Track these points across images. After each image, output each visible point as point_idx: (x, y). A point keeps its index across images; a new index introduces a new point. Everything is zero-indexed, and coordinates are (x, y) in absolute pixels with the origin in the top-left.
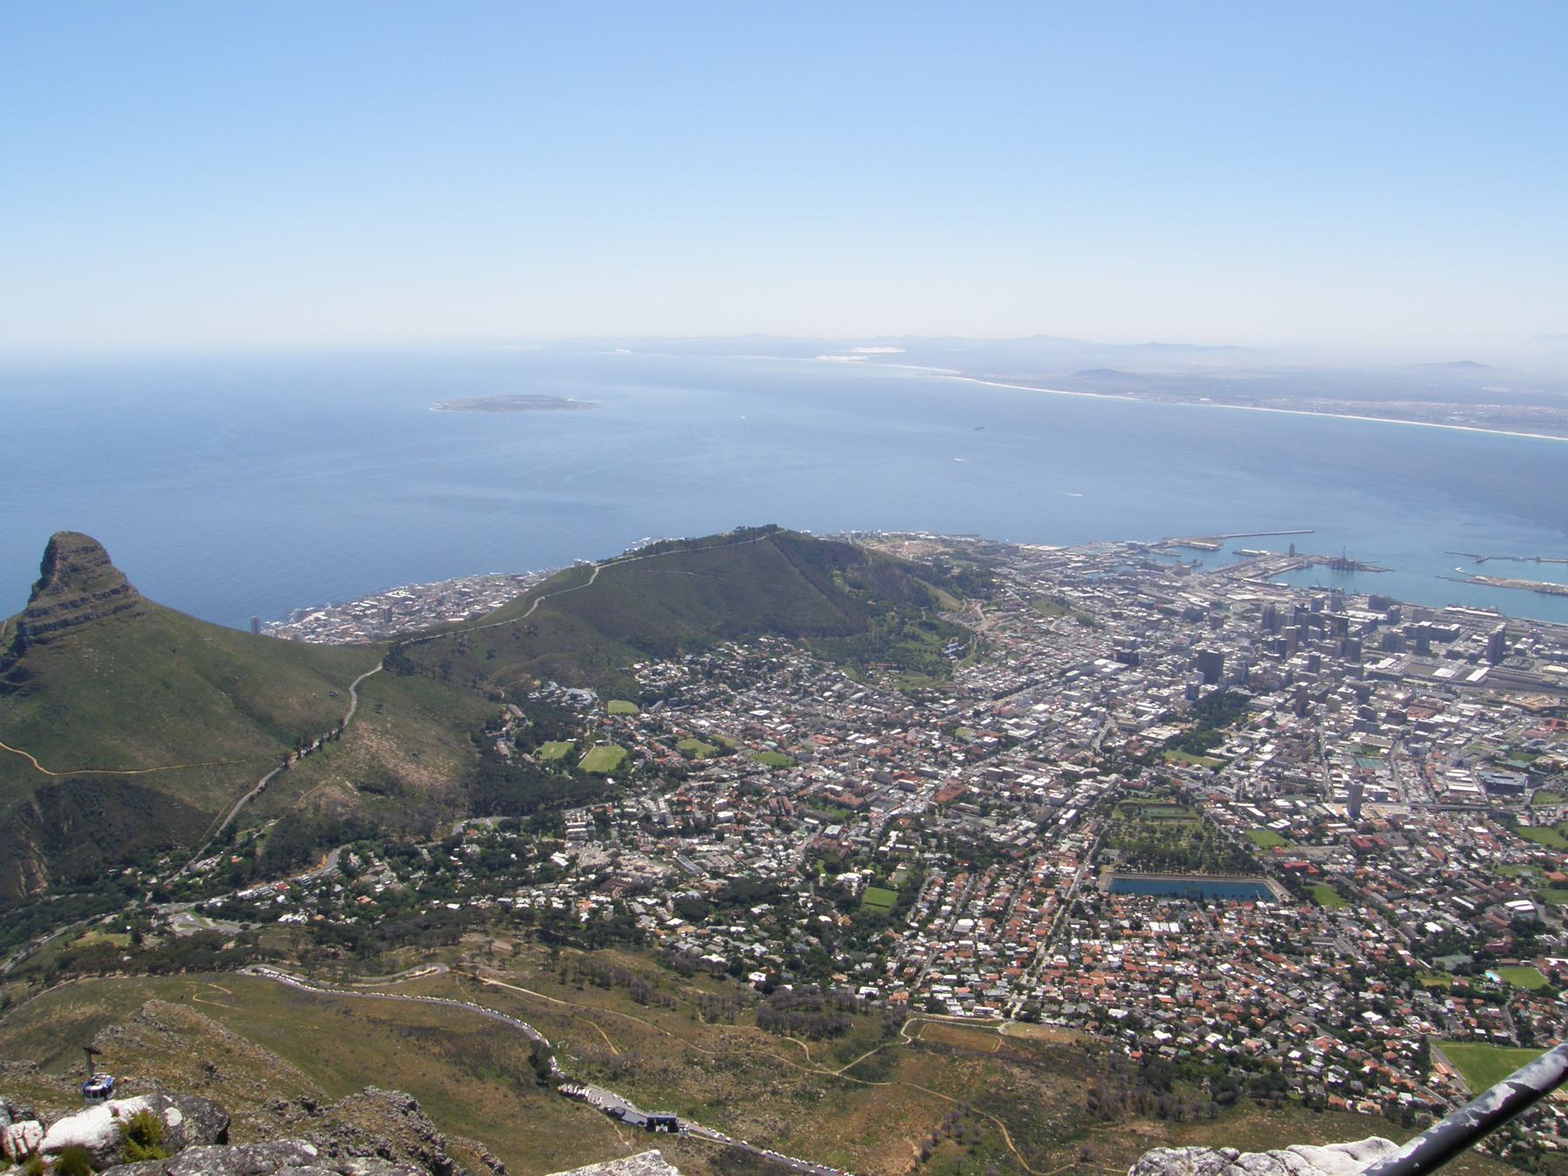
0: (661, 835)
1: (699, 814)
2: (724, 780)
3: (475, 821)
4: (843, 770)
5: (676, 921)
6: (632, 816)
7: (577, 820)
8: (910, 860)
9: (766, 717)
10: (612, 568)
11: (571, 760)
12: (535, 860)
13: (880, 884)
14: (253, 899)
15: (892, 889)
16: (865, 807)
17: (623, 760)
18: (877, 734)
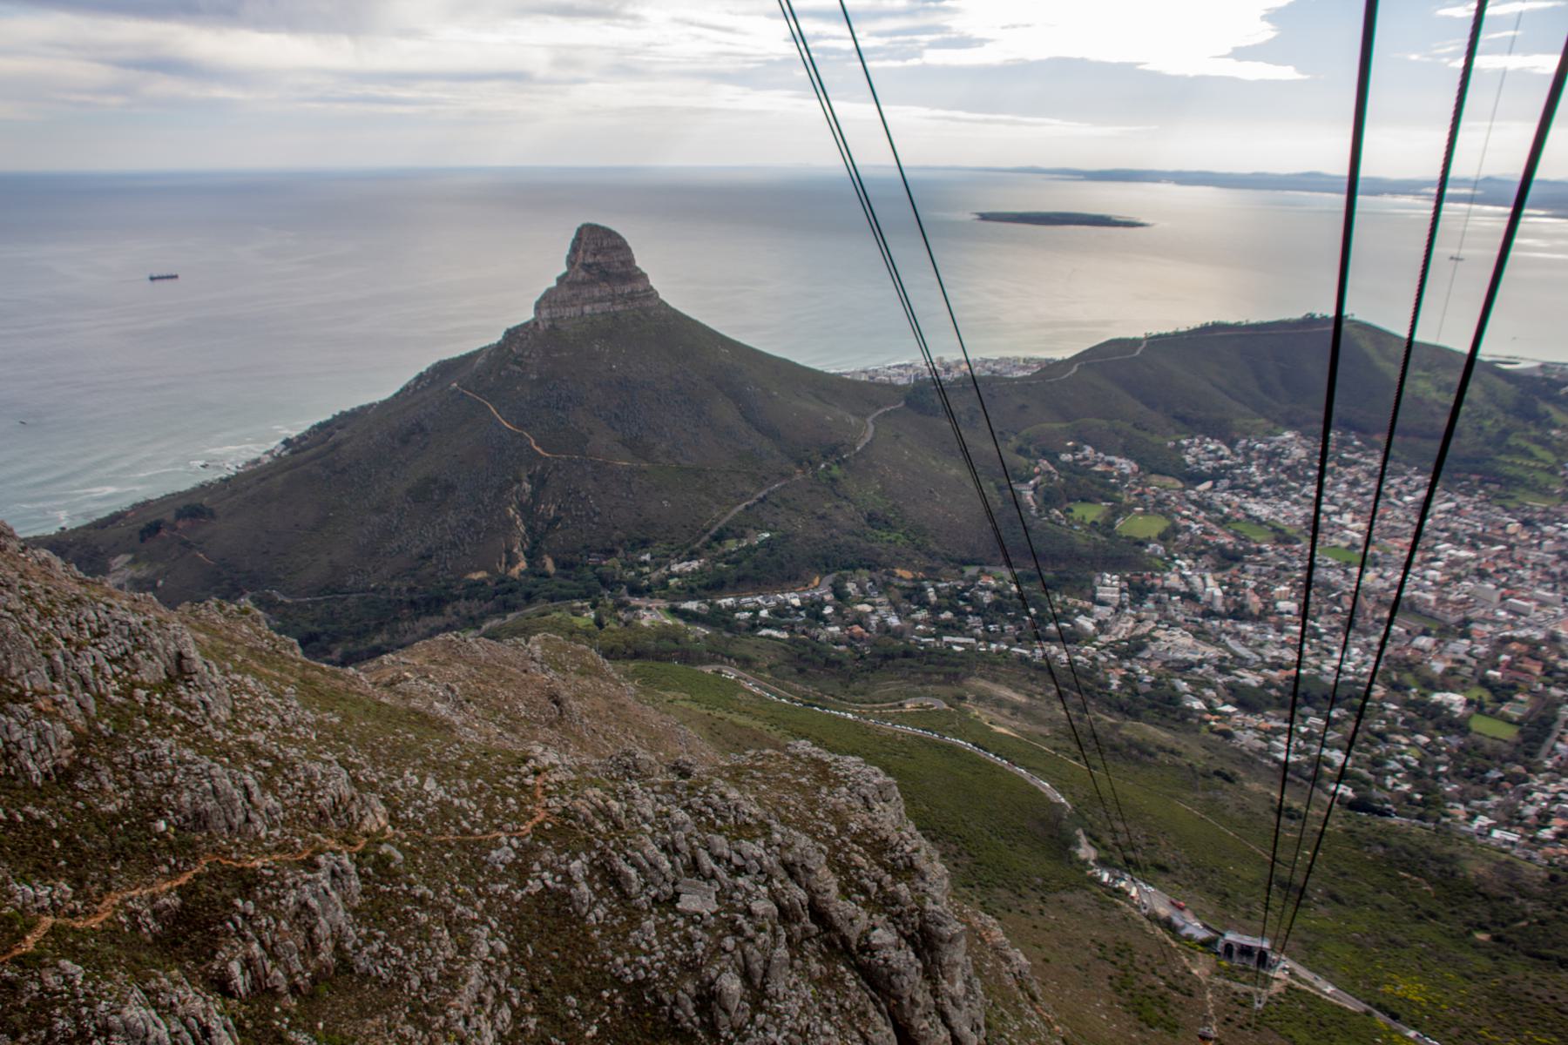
0: (1209, 614)
1: (1256, 599)
2: (1285, 568)
3: (987, 569)
4: (1435, 583)
5: (1229, 709)
6: (1172, 591)
7: (1110, 586)
8: (1530, 692)
9: (1334, 513)
10: (1158, 342)
11: (1107, 527)
12: (1056, 619)
13: (1493, 714)
14: (733, 610)
15: (1509, 721)
16: (1466, 622)
17: (1167, 530)
18: (1473, 547)
